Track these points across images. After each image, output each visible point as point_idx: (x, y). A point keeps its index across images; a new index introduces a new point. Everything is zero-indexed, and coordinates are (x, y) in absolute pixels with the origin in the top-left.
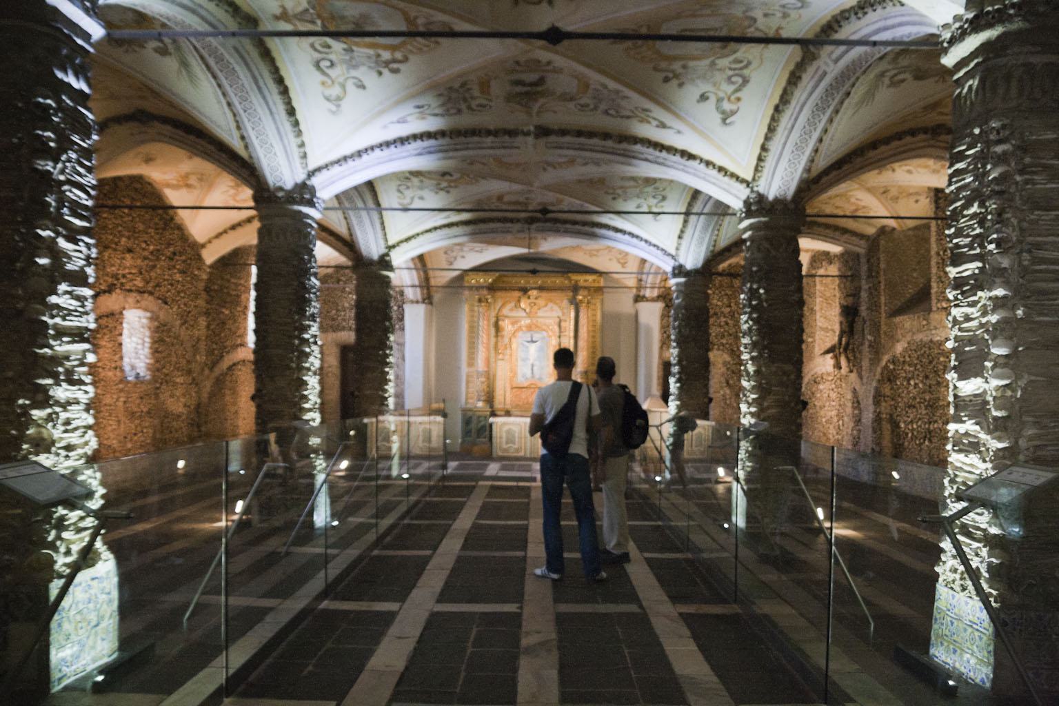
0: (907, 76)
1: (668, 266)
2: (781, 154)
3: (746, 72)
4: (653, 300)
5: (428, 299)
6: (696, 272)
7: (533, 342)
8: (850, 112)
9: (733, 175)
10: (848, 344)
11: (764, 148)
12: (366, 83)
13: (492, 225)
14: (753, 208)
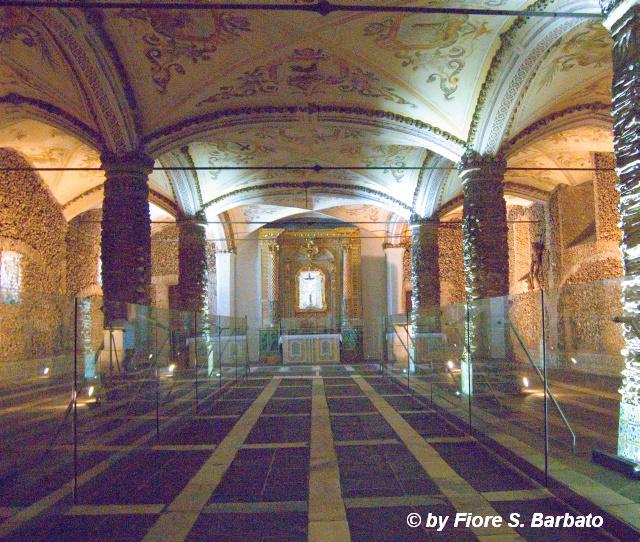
0: (575, 62)
1: (407, 215)
2: (488, 120)
3: (461, 58)
4: (397, 246)
5: (233, 249)
6: (427, 220)
7: (310, 278)
8: (535, 91)
9: (453, 138)
10: (538, 270)
11: (475, 117)
12: (185, 69)
13: (278, 189)
14: (469, 161)
